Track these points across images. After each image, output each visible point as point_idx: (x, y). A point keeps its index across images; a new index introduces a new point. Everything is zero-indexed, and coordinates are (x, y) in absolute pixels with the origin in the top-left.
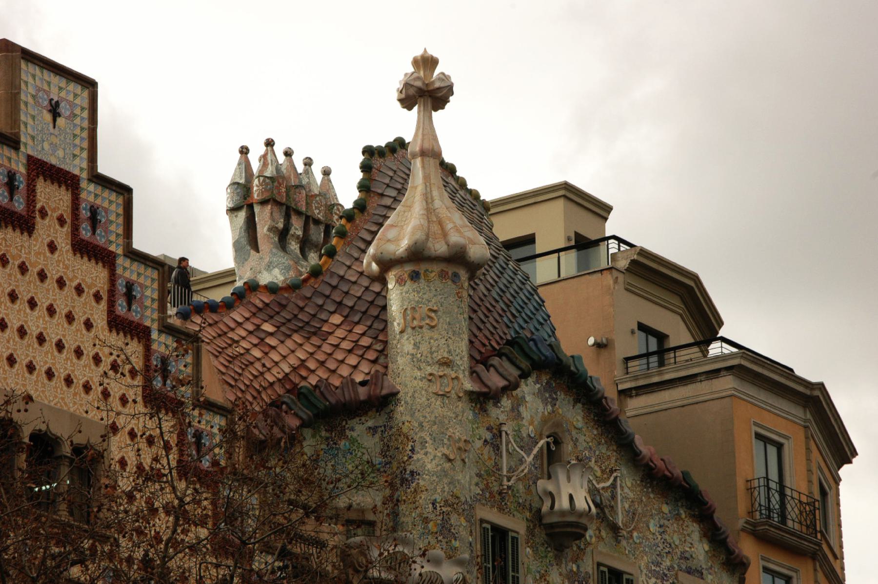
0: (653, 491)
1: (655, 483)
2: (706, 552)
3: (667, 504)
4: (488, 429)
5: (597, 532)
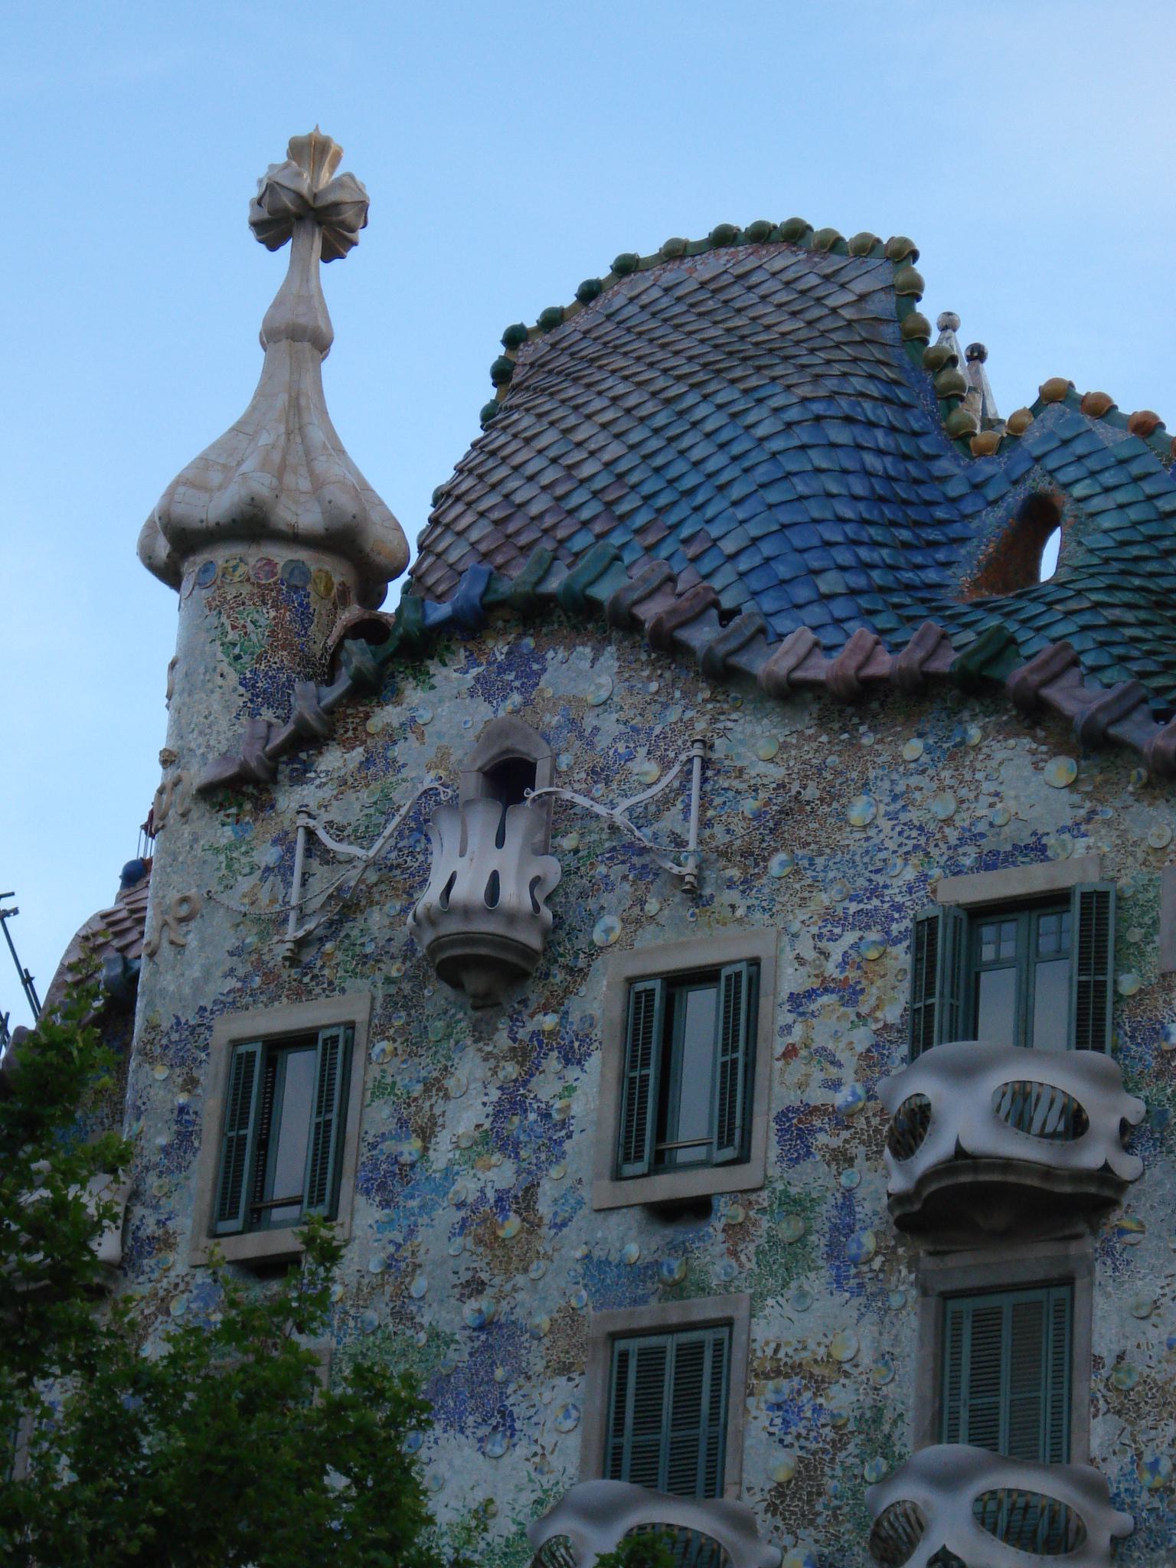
0: (873, 729)
2: (1072, 786)
3: (920, 735)
4: (276, 842)
5: (636, 910)
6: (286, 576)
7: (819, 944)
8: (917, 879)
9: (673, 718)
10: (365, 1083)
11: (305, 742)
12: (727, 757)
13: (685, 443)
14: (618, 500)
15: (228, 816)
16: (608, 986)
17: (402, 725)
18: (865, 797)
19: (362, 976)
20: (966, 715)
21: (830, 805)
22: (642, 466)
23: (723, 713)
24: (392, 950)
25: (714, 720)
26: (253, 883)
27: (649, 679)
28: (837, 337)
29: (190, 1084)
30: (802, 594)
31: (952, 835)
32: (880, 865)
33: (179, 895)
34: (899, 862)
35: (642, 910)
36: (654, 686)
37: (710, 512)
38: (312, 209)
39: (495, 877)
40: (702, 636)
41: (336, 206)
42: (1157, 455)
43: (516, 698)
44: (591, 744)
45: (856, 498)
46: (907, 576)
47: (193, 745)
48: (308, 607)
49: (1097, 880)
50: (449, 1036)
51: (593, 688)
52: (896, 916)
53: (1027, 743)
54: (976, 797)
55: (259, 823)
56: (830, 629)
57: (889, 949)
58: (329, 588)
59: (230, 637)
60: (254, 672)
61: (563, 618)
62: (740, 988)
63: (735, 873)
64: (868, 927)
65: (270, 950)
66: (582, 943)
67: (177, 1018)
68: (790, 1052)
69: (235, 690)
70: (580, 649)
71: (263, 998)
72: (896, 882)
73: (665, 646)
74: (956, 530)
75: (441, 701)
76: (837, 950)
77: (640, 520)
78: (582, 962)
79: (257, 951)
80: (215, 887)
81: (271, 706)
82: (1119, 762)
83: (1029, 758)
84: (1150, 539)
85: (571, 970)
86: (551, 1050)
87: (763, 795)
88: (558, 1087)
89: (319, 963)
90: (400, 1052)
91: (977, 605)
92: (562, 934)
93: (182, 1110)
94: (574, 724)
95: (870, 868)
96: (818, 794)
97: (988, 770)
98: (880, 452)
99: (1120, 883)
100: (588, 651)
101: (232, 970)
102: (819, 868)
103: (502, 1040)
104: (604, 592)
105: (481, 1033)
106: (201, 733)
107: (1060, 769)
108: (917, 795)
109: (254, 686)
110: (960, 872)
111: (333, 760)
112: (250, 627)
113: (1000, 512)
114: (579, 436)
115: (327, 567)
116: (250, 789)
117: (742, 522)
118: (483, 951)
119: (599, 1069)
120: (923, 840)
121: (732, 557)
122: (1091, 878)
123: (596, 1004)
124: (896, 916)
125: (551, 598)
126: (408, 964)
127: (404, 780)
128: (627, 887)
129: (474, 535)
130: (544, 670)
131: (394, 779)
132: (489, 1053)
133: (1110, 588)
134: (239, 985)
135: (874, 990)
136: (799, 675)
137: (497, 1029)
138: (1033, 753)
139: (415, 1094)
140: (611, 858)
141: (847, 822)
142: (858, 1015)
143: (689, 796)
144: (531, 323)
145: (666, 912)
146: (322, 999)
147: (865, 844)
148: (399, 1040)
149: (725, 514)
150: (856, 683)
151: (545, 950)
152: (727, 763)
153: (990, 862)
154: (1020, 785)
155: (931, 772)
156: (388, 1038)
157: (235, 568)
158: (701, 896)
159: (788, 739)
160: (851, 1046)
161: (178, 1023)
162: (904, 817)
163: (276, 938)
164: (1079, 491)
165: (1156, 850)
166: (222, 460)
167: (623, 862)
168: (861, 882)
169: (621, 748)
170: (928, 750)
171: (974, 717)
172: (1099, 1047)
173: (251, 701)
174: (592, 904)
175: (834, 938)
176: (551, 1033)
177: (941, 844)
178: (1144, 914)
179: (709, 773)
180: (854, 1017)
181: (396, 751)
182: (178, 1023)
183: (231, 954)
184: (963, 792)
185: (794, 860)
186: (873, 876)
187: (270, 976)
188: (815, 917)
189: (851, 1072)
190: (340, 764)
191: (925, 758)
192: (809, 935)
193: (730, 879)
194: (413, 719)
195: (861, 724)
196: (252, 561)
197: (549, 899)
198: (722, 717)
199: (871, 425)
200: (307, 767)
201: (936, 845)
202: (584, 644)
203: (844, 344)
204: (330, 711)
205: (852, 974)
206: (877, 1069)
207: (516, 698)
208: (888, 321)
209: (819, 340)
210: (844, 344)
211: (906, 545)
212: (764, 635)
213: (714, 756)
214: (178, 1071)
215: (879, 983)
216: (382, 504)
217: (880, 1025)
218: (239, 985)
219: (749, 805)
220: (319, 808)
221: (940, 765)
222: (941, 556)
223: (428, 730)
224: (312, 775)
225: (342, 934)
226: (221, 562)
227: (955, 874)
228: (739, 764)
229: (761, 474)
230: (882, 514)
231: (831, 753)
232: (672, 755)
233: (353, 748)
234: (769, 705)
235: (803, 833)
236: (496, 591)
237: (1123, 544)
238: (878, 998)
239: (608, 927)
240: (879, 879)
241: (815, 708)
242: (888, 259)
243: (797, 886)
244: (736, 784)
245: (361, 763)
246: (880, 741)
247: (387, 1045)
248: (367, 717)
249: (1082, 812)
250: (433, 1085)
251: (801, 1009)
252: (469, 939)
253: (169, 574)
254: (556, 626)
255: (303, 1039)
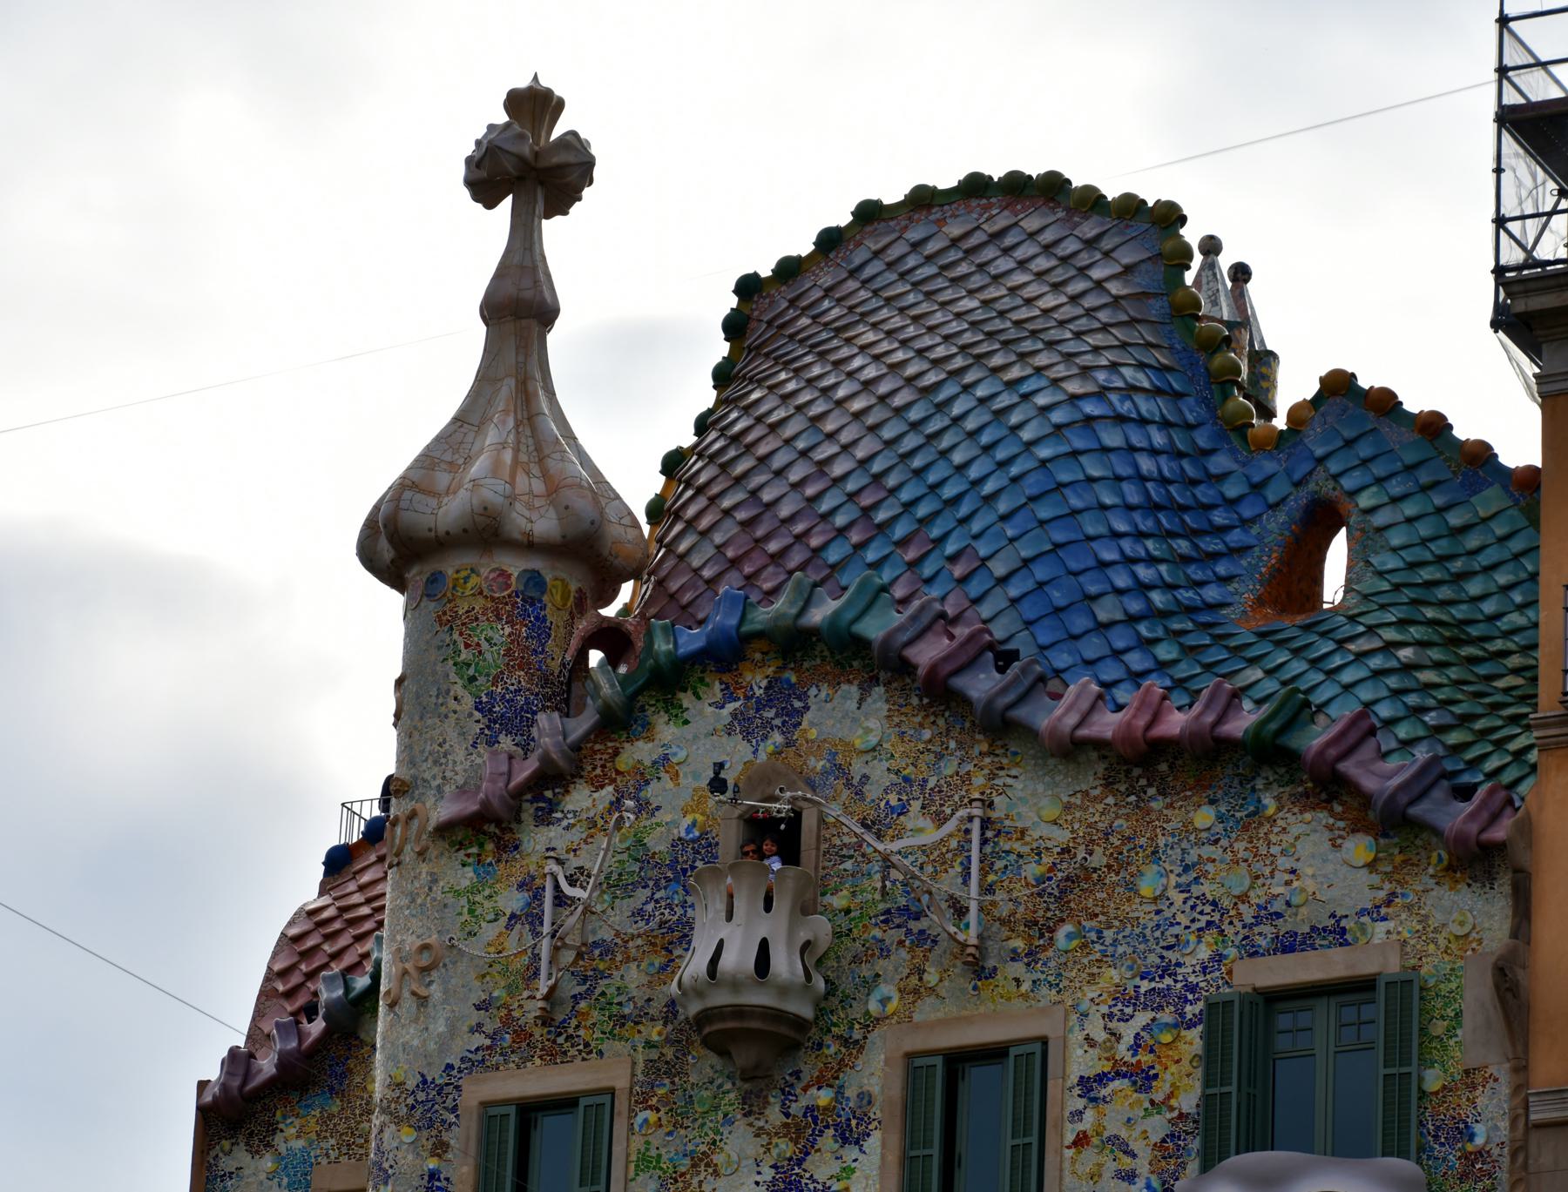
0: (1162, 792)
1: (1163, 767)
2: (1371, 866)
3: (1212, 802)
4: (521, 886)
5: (914, 980)
6: (521, 588)
7: (1110, 1025)
8: (1211, 959)
9: (949, 771)
10: (628, 1155)
11: (549, 783)
12: (1007, 816)
13: (945, 442)
14: (876, 506)
15: (468, 856)
16: (887, 1062)
17: (654, 763)
18: (1155, 867)
19: (620, 1039)
20: (1259, 783)
21: (1117, 874)
22: (901, 466)
23: (1002, 768)
24: (651, 1012)
25: (992, 776)
26: (497, 932)
27: (921, 725)
28: (1104, 316)
29: (439, 1149)
30: (1079, 623)
31: (1248, 913)
32: (1172, 941)
33: (419, 943)
34: (1193, 938)
35: (921, 979)
36: (927, 734)
37: (976, 527)
38: (534, 169)
39: (764, 946)
40: (982, 684)
41: (561, 167)
42: (1446, 460)
43: (777, 738)
44: (859, 793)
45: (1130, 508)
46: (1185, 595)
47: (427, 776)
48: (544, 620)
49: (1397, 969)
50: (717, 1108)
51: (860, 732)
52: (1190, 997)
53: (1323, 816)
54: (1272, 872)
55: (502, 865)
56: (1109, 661)
57: (1183, 1033)
58: (565, 598)
59: (463, 657)
60: (490, 694)
61: (826, 653)
62: (1028, 1062)
63: (1019, 944)
64: (1160, 1008)
65: (521, 1006)
66: (856, 1012)
67: (423, 1076)
68: (1081, 1141)
69: (470, 715)
70: (844, 687)
71: (515, 1058)
72: (1189, 961)
73: (938, 693)
74: (1235, 537)
75: (696, 738)
76: (1128, 1032)
77: (900, 531)
78: (857, 1034)
79: (505, 1006)
80: (457, 934)
81: (509, 733)
82: (1418, 842)
83: (1327, 835)
84: (1441, 560)
85: (846, 1042)
86: (827, 1127)
87: (1047, 860)
88: (835, 1168)
89: (574, 1022)
90: (664, 1122)
91: (1262, 635)
92: (835, 1001)
93: (433, 1175)
94: (841, 771)
95: (1163, 944)
96: (1105, 861)
97: (1284, 845)
98: (1154, 452)
99: (1423, 971)
100: (854, 690)
101: (479, 1025)
102: (1108, 941)
103: (774, 1115)
104: (874, 628)
105: (752, 1105)
106: (435, 762)
107: (1359, 848)
108: (1210, 867)
109: (490, 711)
110: (1256, 953)
111: (580, 799)
112: (485, 645)
113: (1282, 518)
114: (829, 427)
115: (563, 575)
116: (492, 828)
117: (1012, 540)
118: (755, 1024)
119: (879, 1151)
120: (1217, 917)
121: (1003, 581)
122: (1392, 965)
123: (874, 1080)
124: (1190, 997)
125: (813, 632)
126: (670, 1027)
127: (658, 825)
128: (903, 953)
129: (718, 538)
130: (807, 708)
131: (648, 823)
132: (761, 1128)
133: (1402, 624)
134: (488, 1042)
135: (1168, 1076)
136: (1083, 732)
137: (768, 1103)
138: (1330, 828)
139: (683, 1169)
140: (885, 922)
141: (1137, 892)
142: (1152, 1102)
143: (969, 858)
144: (765, 272)
145: (946, 983)
146: (578, 1061)
147: (1156, 918)
148: (663, 1110)
149: (992, 530)
150: (1144, 747)
151: (817, 1018)
152: (1007, 823)
153: (1287, 945)
154: (1321, 864)
155: (1224, 842)
156: (651, 1108)
157: (466, 579)
158: (983, 968)
159: (1073, 800)
160: (1145, 1135)
161: (425, 1082)
162: (1196, 890)
163: (526, 994)
164: (1365, 501)
165: (1457, 937)
166: (448, 457)
167: (899, 926)
168: (1153, 959)
169: (894, 802)
170: (1221, 818)
171: (1268, 785)
172: (1403, 1153)
173: (489, 727)
174: (865, 971)
175: (1126, 1019)
176: (825, 1109)
177: (1236, 921)
178: (1446, 1005)
179: (989, 834)
180: (1147, 1105)
181: (651, 792)
182: (425, 1082)
183: (478, 1008)
184: (1257, 866)
185: (1080, 933)
186: (1165, 953)
187: (522, 1035)
188: (1105, 995)
189: (1146, 1163)
190: (589, 803)
191: (1219, 828)
192: (1099, 1015)
193: (1014, 951)
194: (666, 758)
195: (1150, 785)
196: (484, 572)
197: (819, 962)
198: (1002, 773)
199: (1143, 422)
200: (553, 806)
201: (1231, 923)
202: (850, 682)
203: (1112, 325)
204: (576, 747)
205: (1145, 1058)
206: (1172, 1161)
207: (777, 738)
208: (1156, 295)
209: (1084, 321)
210: (1112, 325)
211: (1186, 560)
212: (1044, 683)
213: (994, 815)
214: (425, 1133)
215: (1173, 1068)
216: (618, 497)
217: (1175, 1114)
218: (488, 1042)
219: (1032, 870)
220: (568, 852)
221: (1234, 835)
222: (1222, 569)
223: (683, 770)
224: (559, 815)
225: (598, 991)
226: (450, 572)
227: (1251, 955)
228: (1019, 825)
229: (1031, 486)
230: (1158, 522)
231: (1117, 817)
232: (948, 811)
233: (602, 787)
234: (1052, 762)
235: (1090, 903)
236: (752, 622)
237: (1413, 566)
238: (1173, 1085)
239: (886, 996)
240: (1172, 956)
241: (1101, 768)
242: (1154, 223)
243: (1085, 961)
244: (1017, 846)
245: (612, 803)
246: (1170, 806)
247: (652, 1116)
248: (616, 753)
249: (1382, 894)
250: (701, 1160)
251: (1092, 1094)
252: (739, 1012)
253: (391, 575)
254: (818, 661)
255: (564, 1103)
